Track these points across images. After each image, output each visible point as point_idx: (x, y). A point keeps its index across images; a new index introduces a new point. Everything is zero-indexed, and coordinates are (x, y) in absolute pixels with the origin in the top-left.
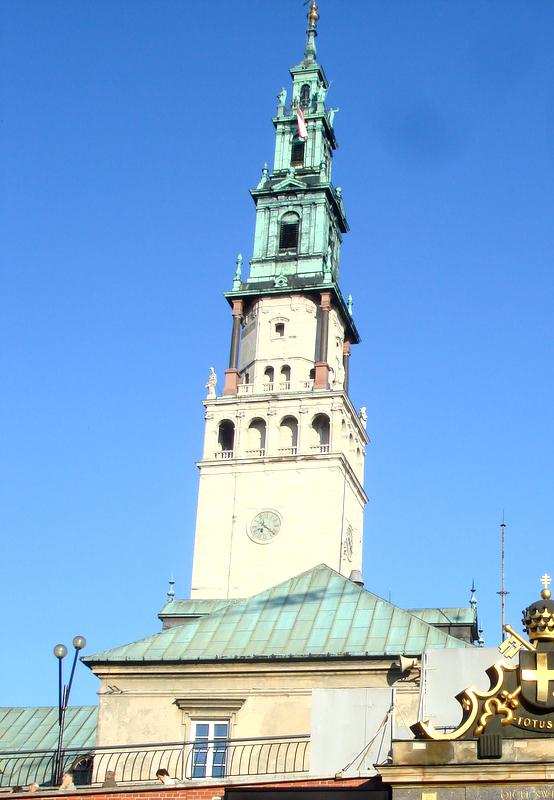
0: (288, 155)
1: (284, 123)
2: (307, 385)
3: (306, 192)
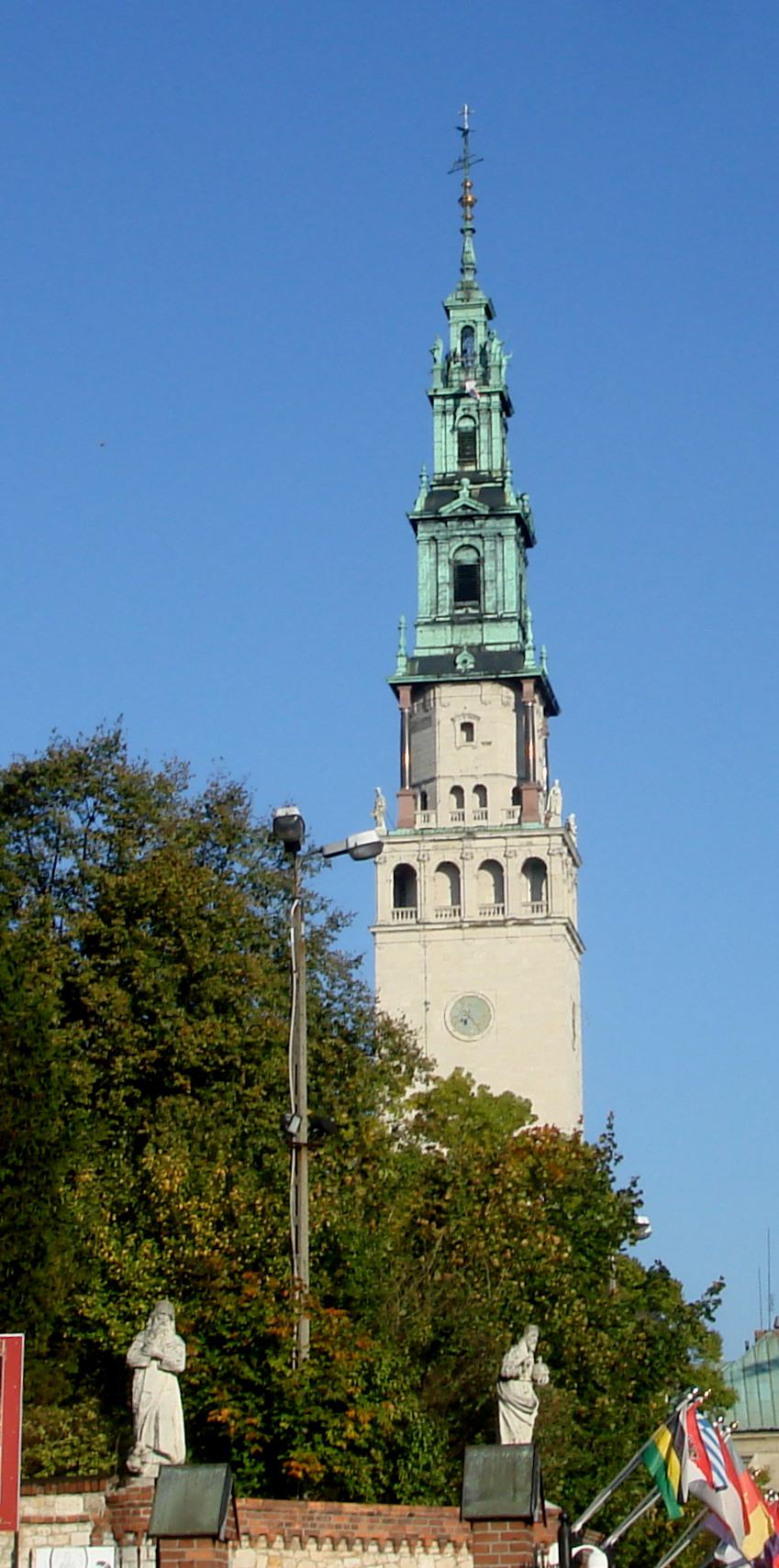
0: (453, 449)
1: (444, 397)
2: (511, 814)
3: (487, 517)
